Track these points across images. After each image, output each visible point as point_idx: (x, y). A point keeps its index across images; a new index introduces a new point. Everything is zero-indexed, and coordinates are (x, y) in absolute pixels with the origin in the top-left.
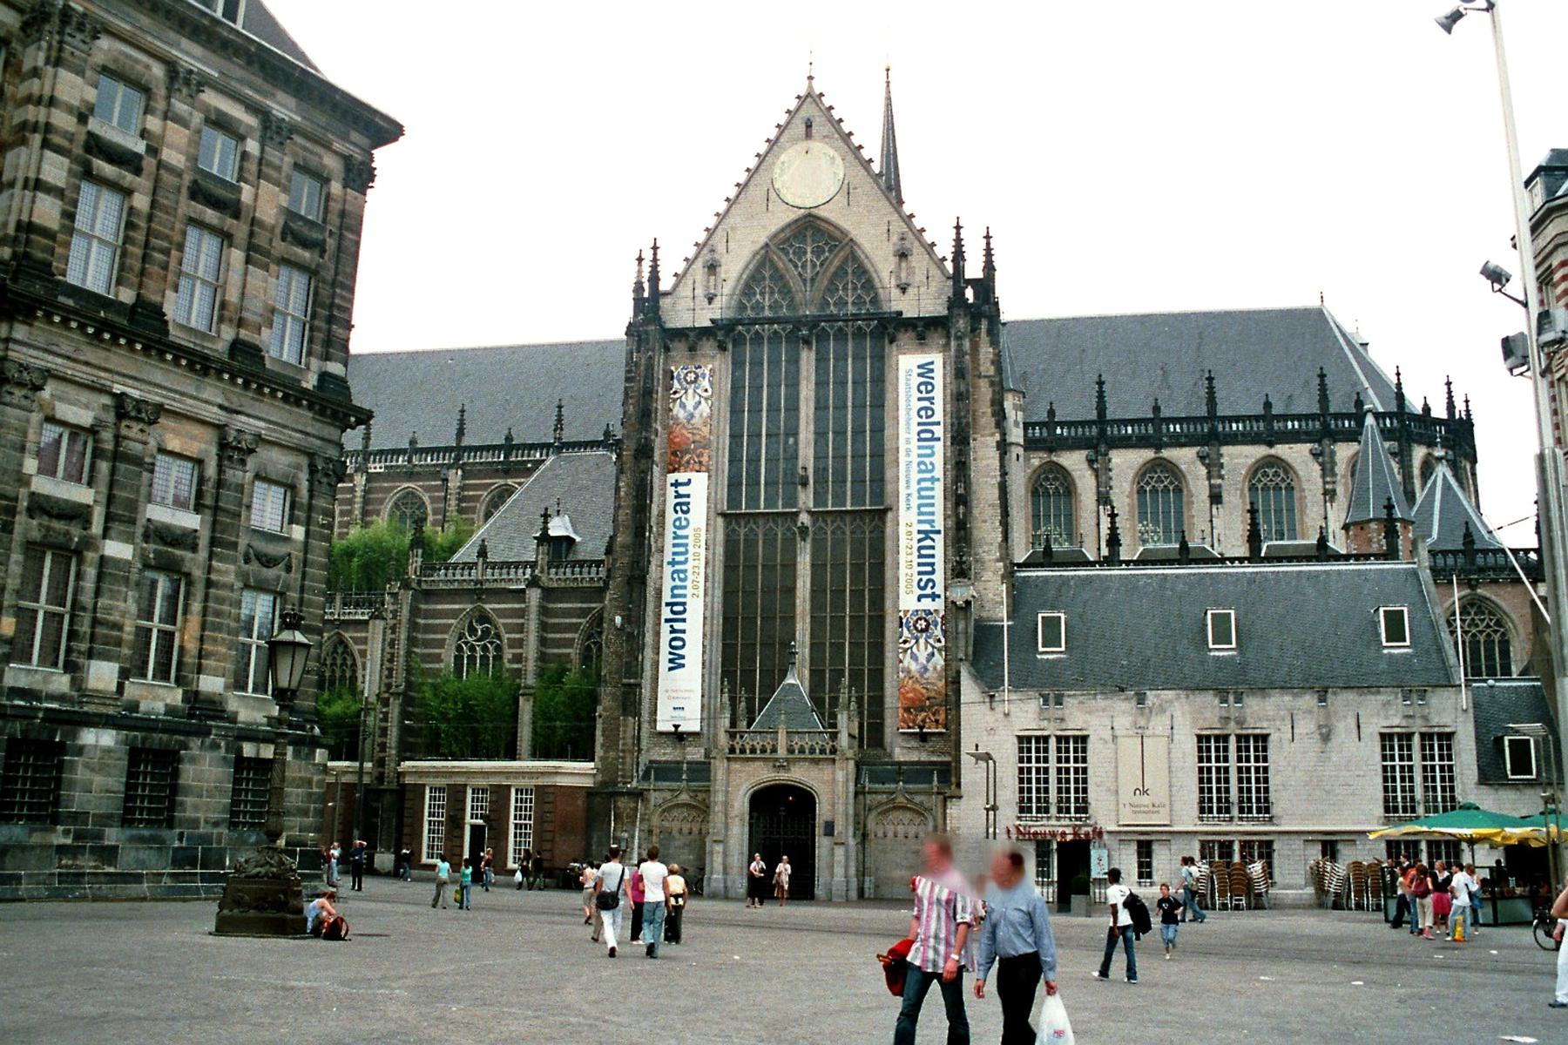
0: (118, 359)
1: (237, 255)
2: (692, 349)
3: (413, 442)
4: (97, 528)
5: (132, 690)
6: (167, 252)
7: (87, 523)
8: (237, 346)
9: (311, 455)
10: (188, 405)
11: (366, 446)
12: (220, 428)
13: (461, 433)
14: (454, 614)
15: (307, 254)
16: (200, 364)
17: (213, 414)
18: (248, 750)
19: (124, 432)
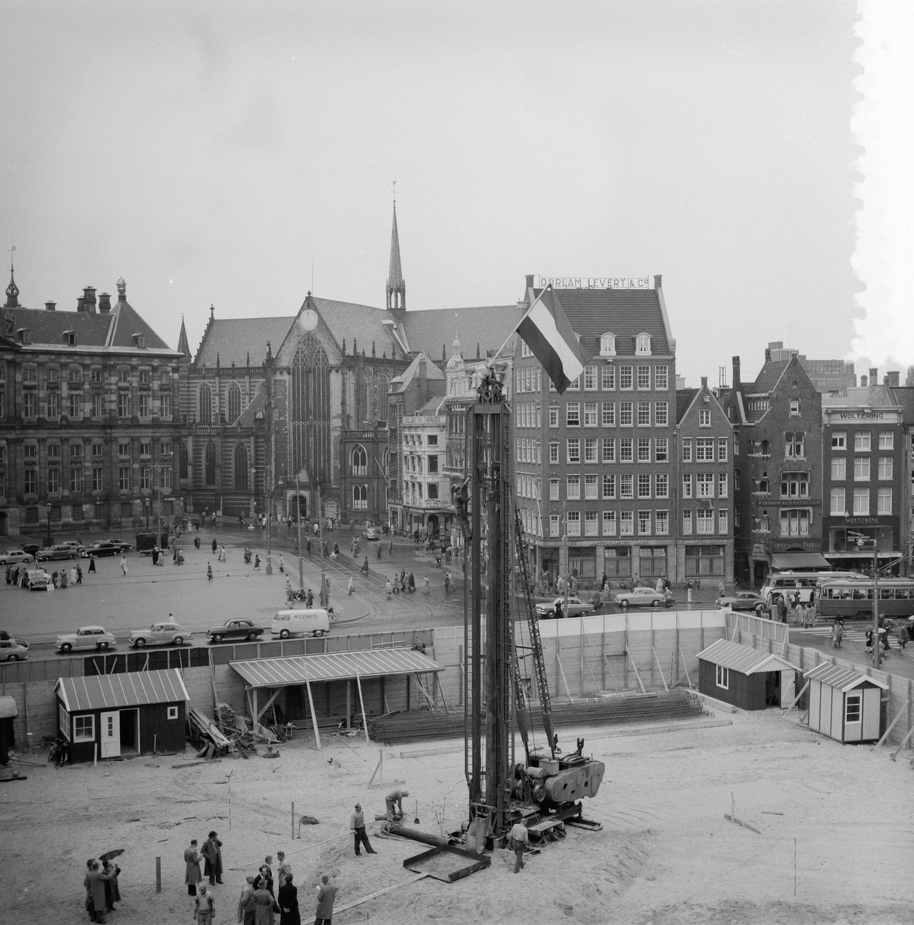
0: (131, 430)
1: (151, 399)
2: (281, 373)
3: (233, 365)
4: (131, 462)
7: (130, 462)
8: (153, 419)
9: (173, 436)
10: (146, 434)
11: (218, 366)
12: (152, 437)
13: (248, 362)
14: (234, 442)
16: (145, 426)
17: (150, 434)
18: (166, 499)
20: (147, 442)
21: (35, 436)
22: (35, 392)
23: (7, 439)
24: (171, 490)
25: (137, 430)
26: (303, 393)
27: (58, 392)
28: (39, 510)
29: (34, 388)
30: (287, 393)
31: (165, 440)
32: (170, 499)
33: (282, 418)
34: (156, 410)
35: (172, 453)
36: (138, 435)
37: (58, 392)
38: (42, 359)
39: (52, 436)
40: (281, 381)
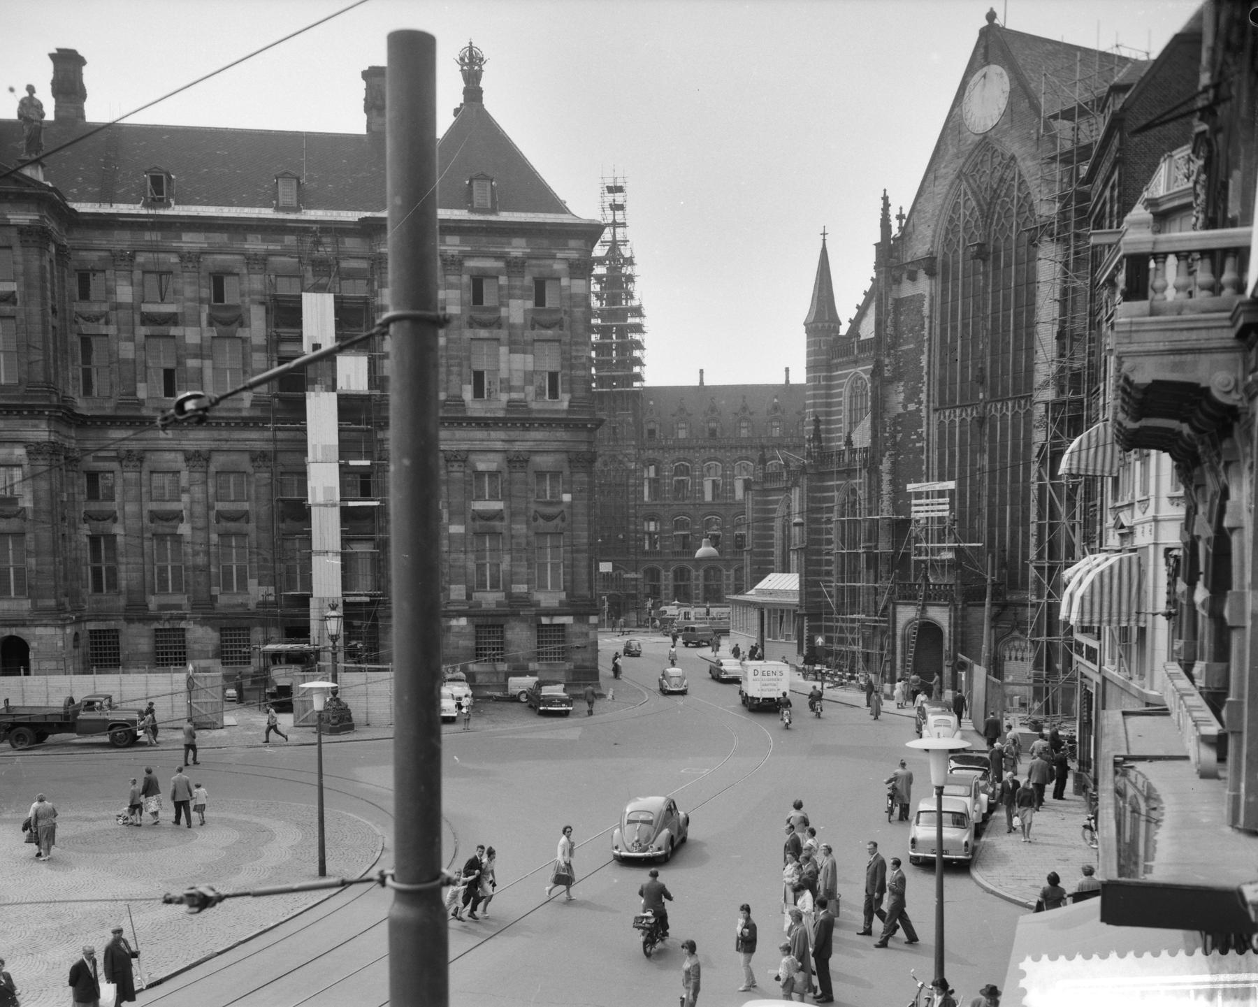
1: (504, 350)
2: (913, 277)
5: (477, 596)
6: (460, 365)
9: (567, 452)
10: (486, 445)
15: (549, 333)
16: (483, 423)
18: (545, 621)
19: (450, 469)
20: (493, 467)
21: (174, 445)
22: (174, 331)
23: (25, 444)
24: (563, 596)
25: (459, 434)
26: (965, 326)
27: (241, 332)
28: (188, 636)
29: (172, 319)
30: (926, 333)
31: (544, 461)
32: (558, 620)
33: (912, 407)
34: (517, 381)
35: (567, 498)
36: (464, 446)
37: (241, 332)
38: (191, 241)
39: (225, 446)
40: (911, 299)
